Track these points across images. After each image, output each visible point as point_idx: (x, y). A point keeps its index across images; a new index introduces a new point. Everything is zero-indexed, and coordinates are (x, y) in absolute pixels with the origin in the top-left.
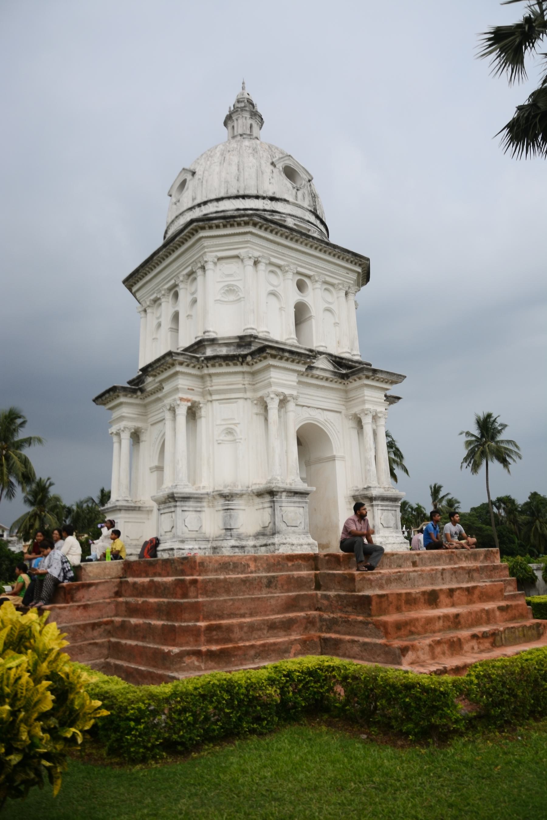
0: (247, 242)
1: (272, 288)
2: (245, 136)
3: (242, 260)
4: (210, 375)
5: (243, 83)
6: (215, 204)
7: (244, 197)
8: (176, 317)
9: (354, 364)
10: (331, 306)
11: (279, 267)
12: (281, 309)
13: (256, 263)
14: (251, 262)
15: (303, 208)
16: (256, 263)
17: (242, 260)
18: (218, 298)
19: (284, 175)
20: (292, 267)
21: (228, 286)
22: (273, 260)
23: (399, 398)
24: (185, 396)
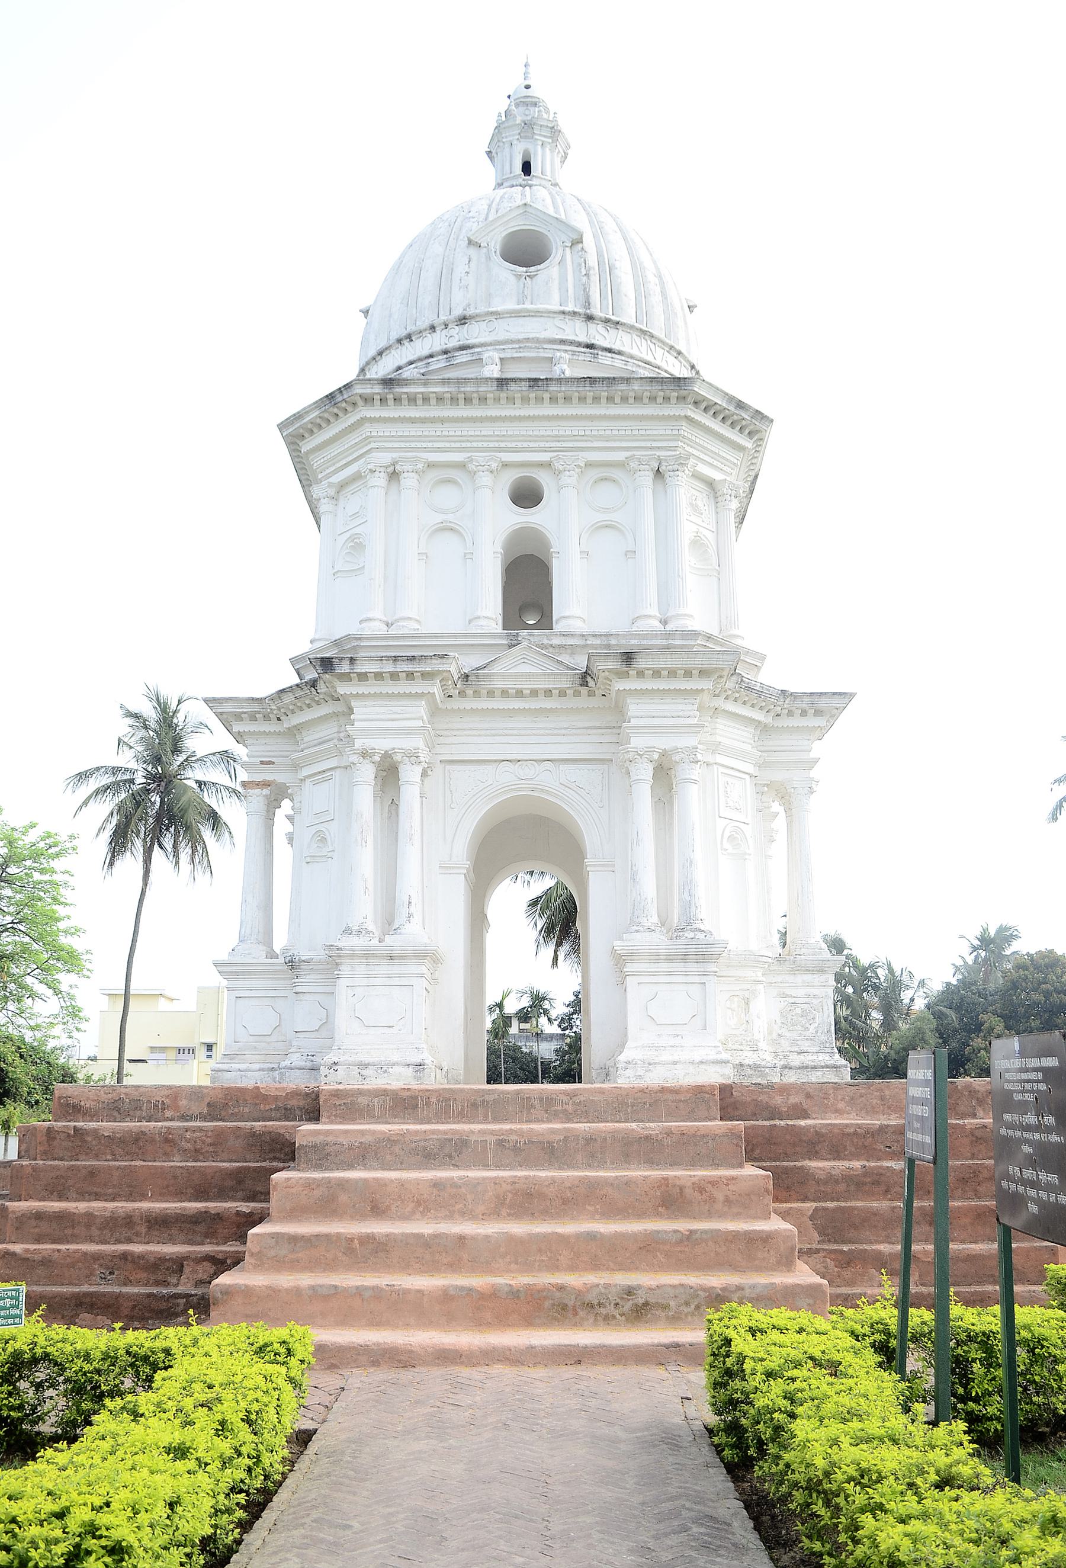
1: (440, 518)
4: (299, 728)
9: (645, 642)
11: (462, 466)
13: (394, 476)
16: (394, 476)
21: (352, 538)
23: (847, 697)
24: (258, 778)
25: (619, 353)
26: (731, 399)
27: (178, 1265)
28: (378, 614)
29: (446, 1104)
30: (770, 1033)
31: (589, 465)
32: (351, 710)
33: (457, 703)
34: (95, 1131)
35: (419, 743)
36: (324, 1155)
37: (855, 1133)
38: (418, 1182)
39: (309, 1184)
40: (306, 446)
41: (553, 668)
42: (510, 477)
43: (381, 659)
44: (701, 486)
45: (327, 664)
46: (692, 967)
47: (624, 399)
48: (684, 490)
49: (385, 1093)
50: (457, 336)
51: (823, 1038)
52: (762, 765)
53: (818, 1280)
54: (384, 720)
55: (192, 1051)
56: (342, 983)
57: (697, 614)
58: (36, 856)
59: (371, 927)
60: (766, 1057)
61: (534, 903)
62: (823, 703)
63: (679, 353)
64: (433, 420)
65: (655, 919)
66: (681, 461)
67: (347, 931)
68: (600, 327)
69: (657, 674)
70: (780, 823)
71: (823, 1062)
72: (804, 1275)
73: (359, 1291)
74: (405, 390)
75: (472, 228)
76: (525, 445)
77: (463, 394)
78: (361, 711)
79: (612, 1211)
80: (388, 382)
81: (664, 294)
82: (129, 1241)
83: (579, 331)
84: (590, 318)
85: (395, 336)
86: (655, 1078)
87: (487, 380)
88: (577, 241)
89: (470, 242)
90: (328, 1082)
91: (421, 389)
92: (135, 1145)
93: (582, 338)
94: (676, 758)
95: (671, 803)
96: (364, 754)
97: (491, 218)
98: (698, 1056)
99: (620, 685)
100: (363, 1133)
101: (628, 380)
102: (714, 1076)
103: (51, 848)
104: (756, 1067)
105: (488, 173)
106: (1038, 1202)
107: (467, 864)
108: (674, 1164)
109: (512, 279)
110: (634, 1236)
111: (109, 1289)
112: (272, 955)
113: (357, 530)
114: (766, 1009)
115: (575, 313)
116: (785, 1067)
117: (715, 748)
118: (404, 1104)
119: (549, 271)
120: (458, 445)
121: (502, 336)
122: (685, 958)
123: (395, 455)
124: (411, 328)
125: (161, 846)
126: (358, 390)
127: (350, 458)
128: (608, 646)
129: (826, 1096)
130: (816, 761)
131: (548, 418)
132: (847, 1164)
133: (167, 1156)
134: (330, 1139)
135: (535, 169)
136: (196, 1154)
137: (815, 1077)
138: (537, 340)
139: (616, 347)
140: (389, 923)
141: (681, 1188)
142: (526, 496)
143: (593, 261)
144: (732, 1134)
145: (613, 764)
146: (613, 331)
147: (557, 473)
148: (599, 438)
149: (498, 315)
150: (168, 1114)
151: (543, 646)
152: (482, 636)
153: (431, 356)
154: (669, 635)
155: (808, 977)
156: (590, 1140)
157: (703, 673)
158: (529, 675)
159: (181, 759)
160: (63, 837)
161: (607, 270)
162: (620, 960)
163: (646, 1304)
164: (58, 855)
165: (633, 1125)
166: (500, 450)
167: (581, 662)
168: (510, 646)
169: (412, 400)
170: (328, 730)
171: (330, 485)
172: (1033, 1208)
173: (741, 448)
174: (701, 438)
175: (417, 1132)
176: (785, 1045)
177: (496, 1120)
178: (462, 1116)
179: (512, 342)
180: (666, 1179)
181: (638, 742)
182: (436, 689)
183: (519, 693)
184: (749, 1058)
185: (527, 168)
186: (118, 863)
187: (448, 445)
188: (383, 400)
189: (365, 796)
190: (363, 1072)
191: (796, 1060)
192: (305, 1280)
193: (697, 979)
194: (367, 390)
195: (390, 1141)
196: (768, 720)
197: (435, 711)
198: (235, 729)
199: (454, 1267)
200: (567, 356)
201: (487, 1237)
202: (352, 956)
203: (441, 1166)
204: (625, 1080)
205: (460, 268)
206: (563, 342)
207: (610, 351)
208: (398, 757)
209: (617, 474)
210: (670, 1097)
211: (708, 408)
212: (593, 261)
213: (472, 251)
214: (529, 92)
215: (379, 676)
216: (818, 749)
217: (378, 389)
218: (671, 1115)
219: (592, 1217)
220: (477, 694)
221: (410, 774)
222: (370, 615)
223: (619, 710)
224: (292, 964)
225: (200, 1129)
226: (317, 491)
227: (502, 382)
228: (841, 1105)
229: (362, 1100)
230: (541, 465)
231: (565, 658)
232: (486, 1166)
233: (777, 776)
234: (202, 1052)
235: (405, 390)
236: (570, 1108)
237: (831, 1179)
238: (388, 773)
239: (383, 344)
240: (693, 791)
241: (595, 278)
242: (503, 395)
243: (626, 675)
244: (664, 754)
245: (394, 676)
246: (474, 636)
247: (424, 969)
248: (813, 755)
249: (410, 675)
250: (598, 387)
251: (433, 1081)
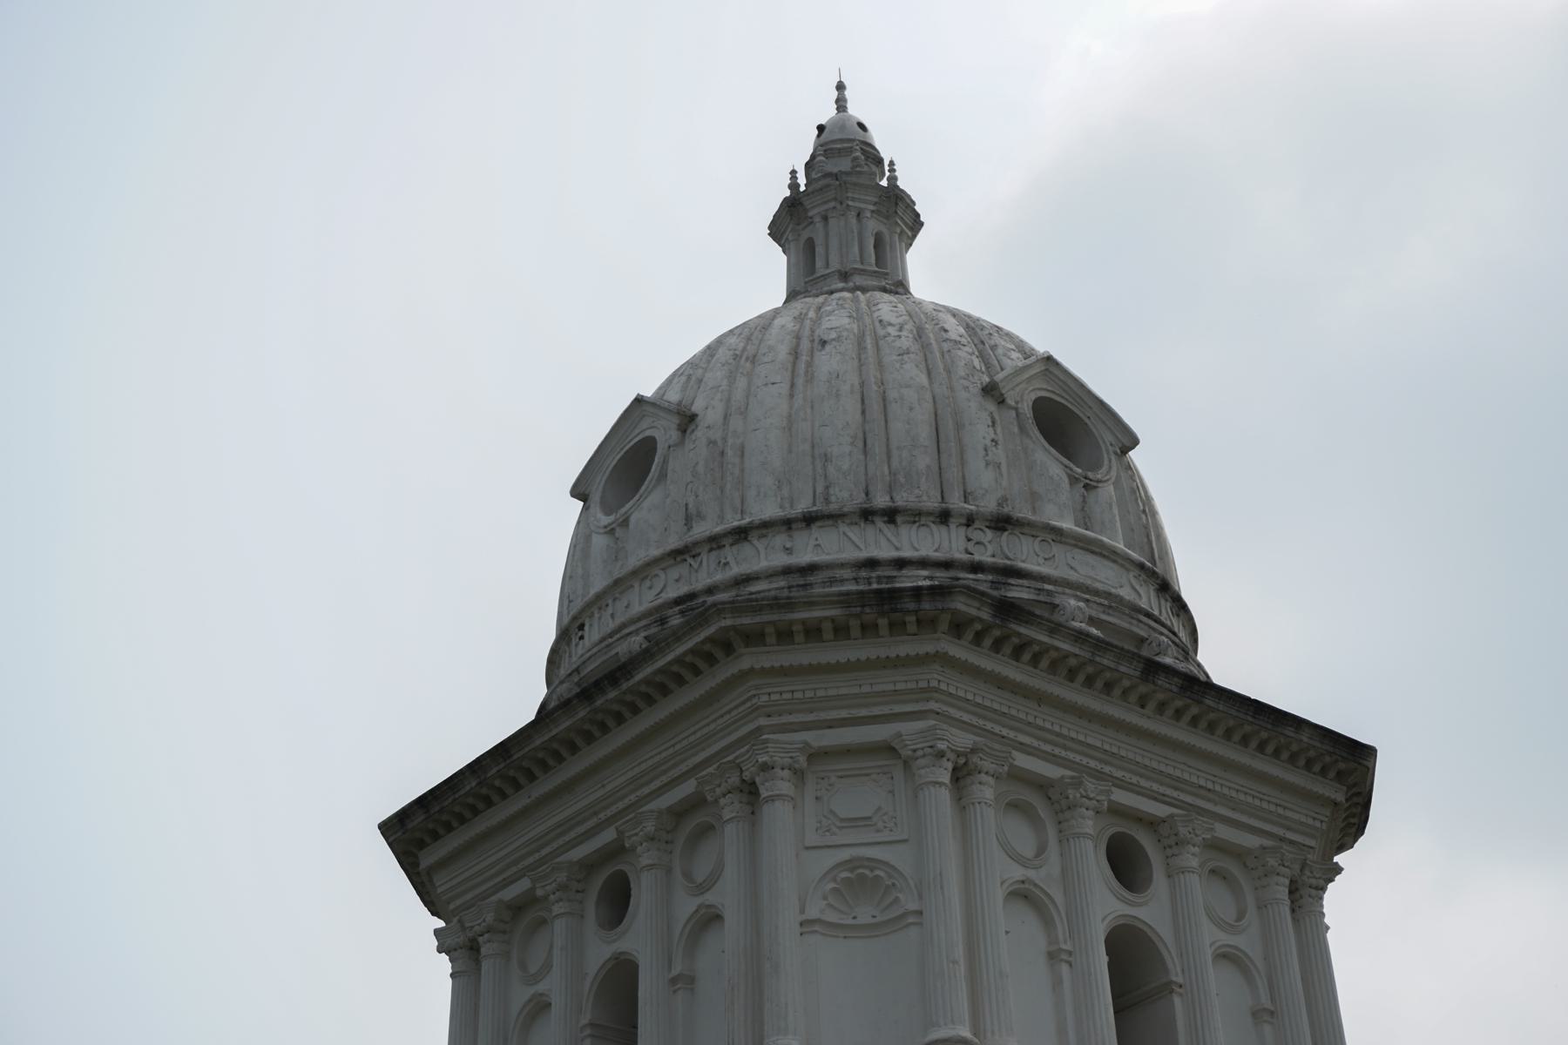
0: (928, 692)
1: (1018, 873)
2: (858, 280)
3: (907, 764)
5: (840, 87)
6: (780, 539)
7: (891, 515)
8: (620, 983)
12: (1053, 956)
13: (960, 775)
15: (1109, 554)
17: (907, 764)
18: (812, 913)
19: (1035, 432)
20: (1090, 785)
21: (851, 864)
22: (1023, 761)
74: (1022, 630)
76: (1135, 779)
85: (846, 496)
120: (1048, 748)
126: (961, 604)
127: (864, 712)
187: (1036, 743)
217: (985, 615)
235: (1022, 630)
239: (803, 505)
242: (1143, 689)
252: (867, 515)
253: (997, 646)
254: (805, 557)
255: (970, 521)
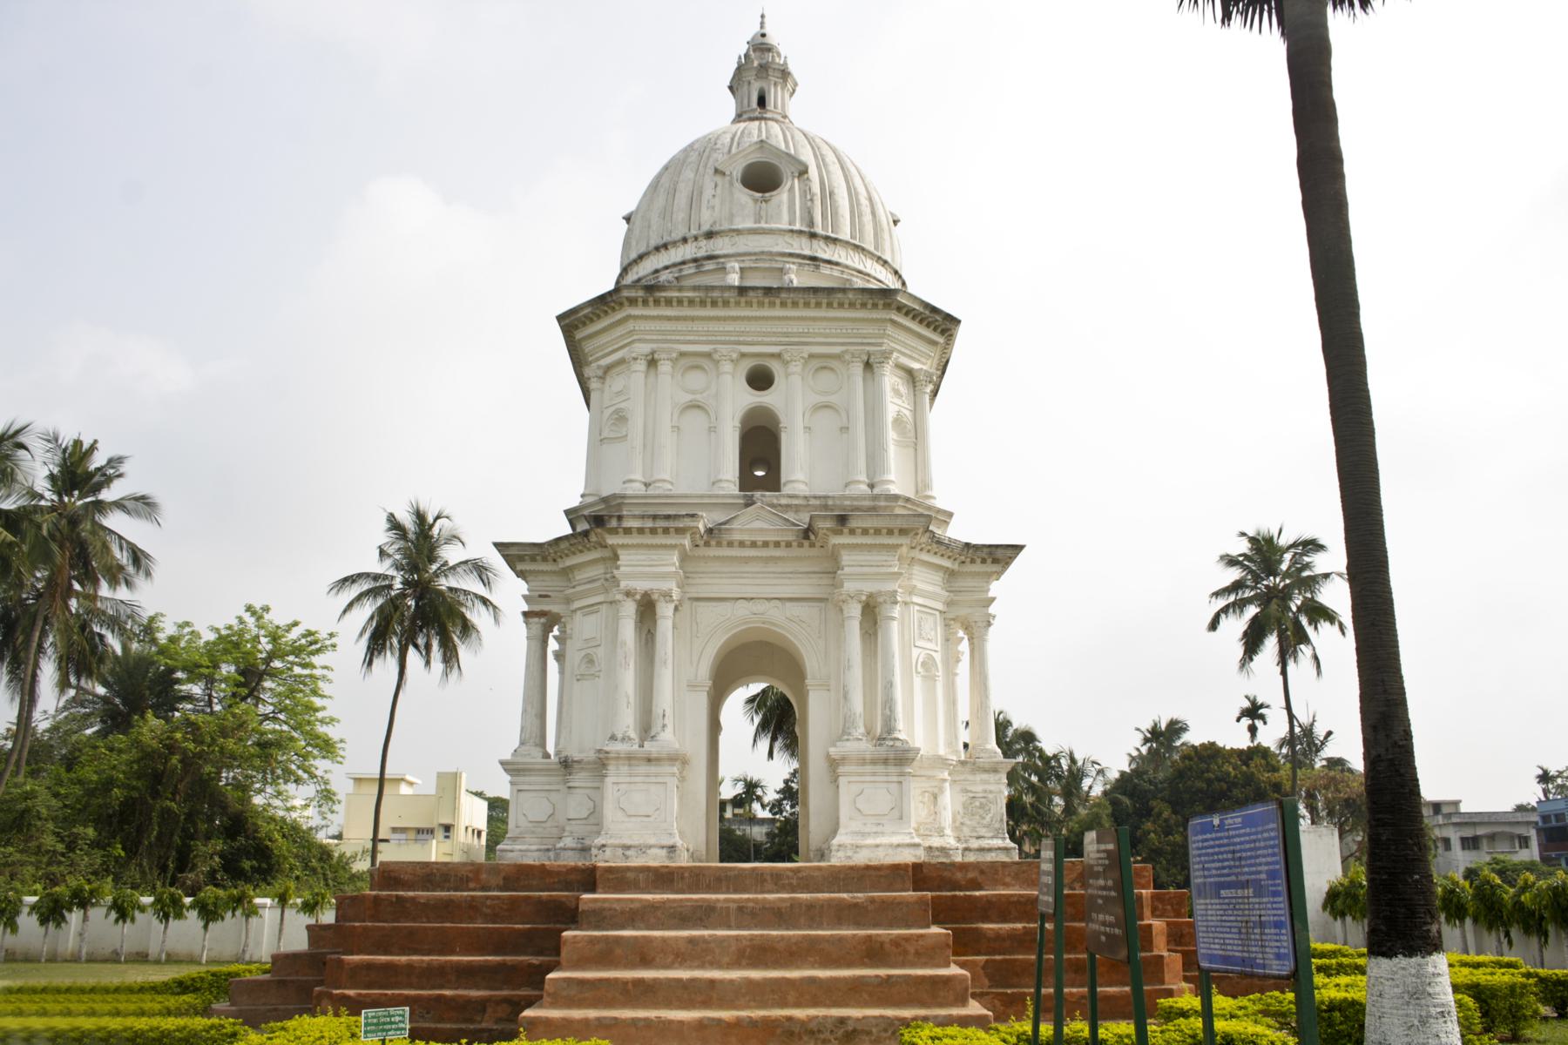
0: (631, 332)
1: (689, 397)
4: (571, 568)
6: (635, 269)
7: (665, 246)
10: (833, 399)
11: (708, 355)
13: (652, 363)
14: (641, 366)
16: (652, 363)
18: (605, 435)
19: (738, 185)
20: (723, 349)
21: (617, 411)
23: (1021, 548)
24: (537, 608)
25: (837, 264)
26: (927, 305)
27: (482, 1005)
28: (638, 476)
29: (693, 878)
30: (954, 821)
31: (811, 356)
32: (616, 557)
33: (703, 551)
34: (413, 899)
35: (672, 586)
36: (601, 918)
37: (1019, 902)
38: (677, 939)
39: (592, 940)
40: (579, 335)
41: (780, 525)
42: (747, 365)
43: (643, 517)
44: (902, 373)
45: (598, 521)
46: (892, 769)
47: (841, 305)
48: (890, 380)
49: (648, 869)
50: (704, 248)
51: (997, 825)
52: (949, 604)
53: (985, 1012)
54: (646, 567)
55: (431, 831)
56: (609, 780)
57: (897, 481)
58: (297, 651)
59: (633, 735)
60: (951, 841)
61: (751, 700)
62: (999, 553)
63: (885, 262)
64: (685, 319)
65: (862, 730)
66: (886, 355)
67: (613, 738)
68: (822, 243)
69: (865, 532)
70: (964, 646)
71: (997, 844)
72: (974, 1008)
73: (634, 1021)
75: (719, 158)
77: (712, 297)
78: (625, 557)
79: (828, 962)
80: (650, 289)
81: (873, 213)
82: (441, 987)
83: (804, 247)
84: (813, 236)
85: (653, 243)
86: (861, 858)
87: (731, 288)
88: (803, 172)
89: (717, 171)
90: (602, 860)
91: (676, 294)
92: (446, 909)
93: (807, 252)
94: (881, 599)
95: (876, 634)
96: (628, 594)
97: (734, 150)
98: (896, 840)
99: (836, 540)
100: (632, 900)
101: (844, 290)
102: (908, 857)
103: (312, 644)
104: (943, 850)
105: (729, 105)
106: (1105, 934)
107: (709, 683)
108: (876, 925)
109: (750, 203)
110: (845, 979)
111: (427, 1025)
112: (547, 756)
113: (622, 405)
114: (949, 801)
115: (801, 232)
116: (966, 849)
117: (912, 591)
118: (663, 878)
119: (781, 196)
121: (742, 249)
122: (886, 761)
123: (654, 346)
124: (667, 239)
125: (416, 646)
128: (826, 507)
129: (996, 872)
130: (993, 599)
131: (779, 318)
132: (1012, 926)
133: (472, 920)
134: (606, 905)
135: (770, 105)
136: (494, 918)
137: (990, 857)
138: (770, 253)
139: (835, 258)
140: (646, 730)
141: (882, 944)
142: (760, 379)
143: (816, 188)
144: (921, 901)
145: (828, 601)
146: (832, 246)
147: (786, 363)
148: (820, 335)
149: (738, 232)
150: (472, 885)
151: (773, 506)
152: (724, 496)
153: (684, 263)
154: (875, 498)
155: (985, 776)
156: (810, 906)
157: (903, 532)
158: (761, 530)
159: (434, 567)
160: (323, 635)
161: (828, 195)
162: (834, 764)
163: (854, 1031)
164: (318, 651)
165: (845, 895)
166: (739, 343)
167: (804, 519)
168: (747, 505)
169: (669, 302)
170: (596, 571)
171: (599, 367)
172: (1103, 938)
173: (935, 343)
174: (902, 336)
175: (674, 901)
176: (966, 831)
177: (736, 891)
178: (709, 889)
179: (750, 254)
180: (870, 937)
181: (849, 587)
182: (687, 542)
183: (754, 544)
184: (936, 842)
185: (762, 102)
186: (376, 662)
188: (645, 303)
189: (628, 630)
190: (628, 853)
191: (975, 844)
192: (592, 1014)
193: (895, 779)
194: (632, 294)
195: (654, 907)
196: (956, 567)
197: (684, 558)
198: (519, 567)
199: (706, 1004)
200: (794, 267)
201: (731, 981)
202: (618, 758)
203: (693, 927)
204: (837, 859)
205: (708, 192)
206: (791, 255)
207: (829, 262)
208: (655, 597)
209: (834, 364)
210: (873, 873)
211: (908, 312)
212: (816, 188)
213: (718, 179)
214: (765, 40)
215: (641, 531)
216: (995, 588)
217: (641, 293)
218: (874, 888)
219: (813, 967)
220: (719, 544)
221: (665, 611)
222: (632, 477)
223: (834, 558)
224: (566, 764)
225: (498, 898)
226: (588, 372)
227: (742, 290)
228: (1008, 880)
229: (630, 875)
230: (772, 355)
231: (791, 516)
232: (729, 928)
233: (963, 612)
234: (440, 834)
236: (794, 882)
237: (998, 936)
238: (647, 609)
239: (643, 249)
240: (895, 625)
241: (818, 202)
242: (743, 300)
243: (840, 533)
244: (870, 596)
245: (653, 531)
246: (717, 496)
247: (675, 770)
248: (991, 594)
249: (666, 531)
250: (820, 295)
251: (683, 861)
252: (657, 249)
253: (657, 302)
254: (641, 274)
255: (696, 238)
